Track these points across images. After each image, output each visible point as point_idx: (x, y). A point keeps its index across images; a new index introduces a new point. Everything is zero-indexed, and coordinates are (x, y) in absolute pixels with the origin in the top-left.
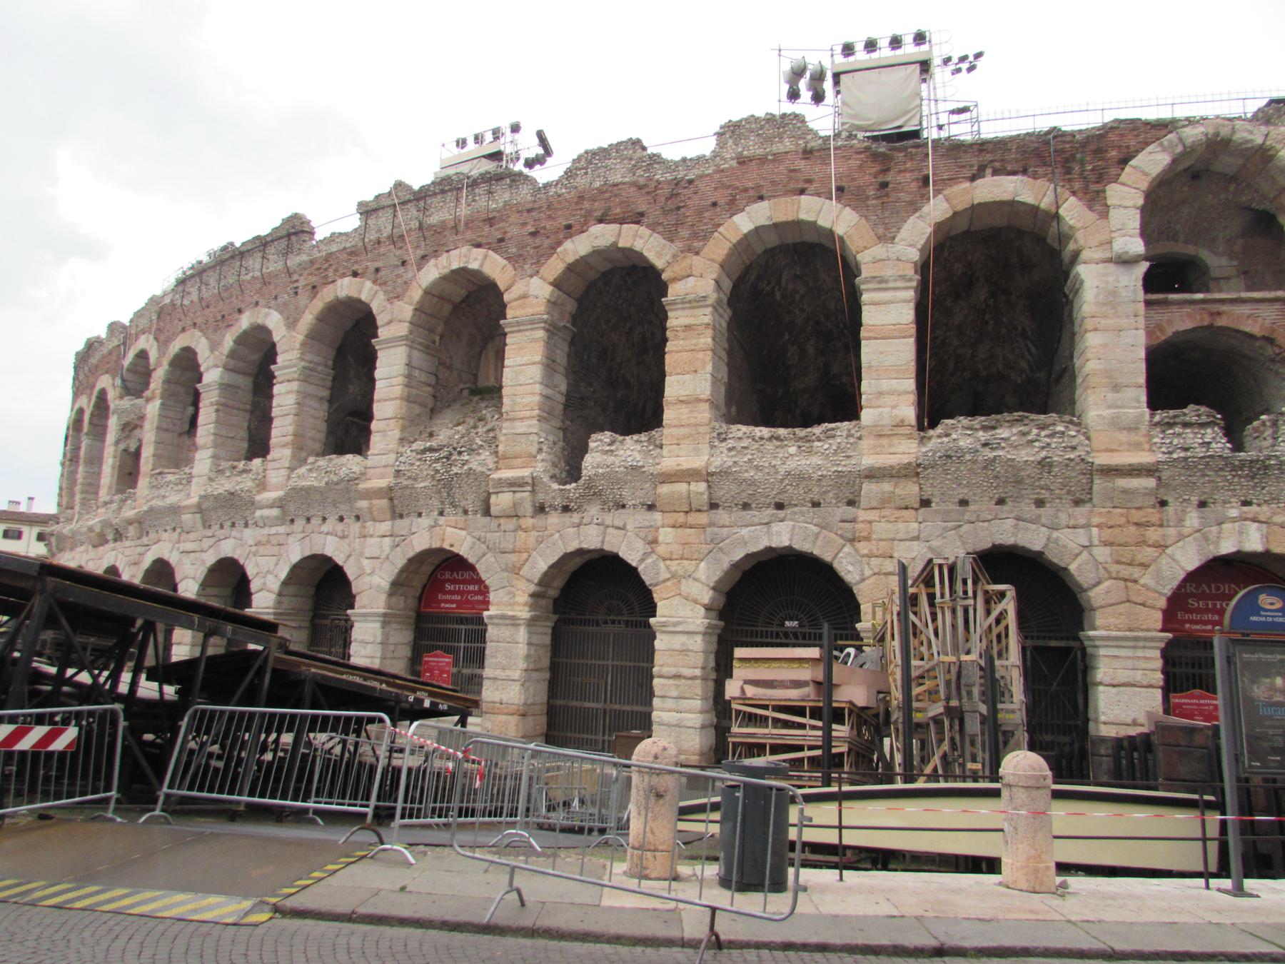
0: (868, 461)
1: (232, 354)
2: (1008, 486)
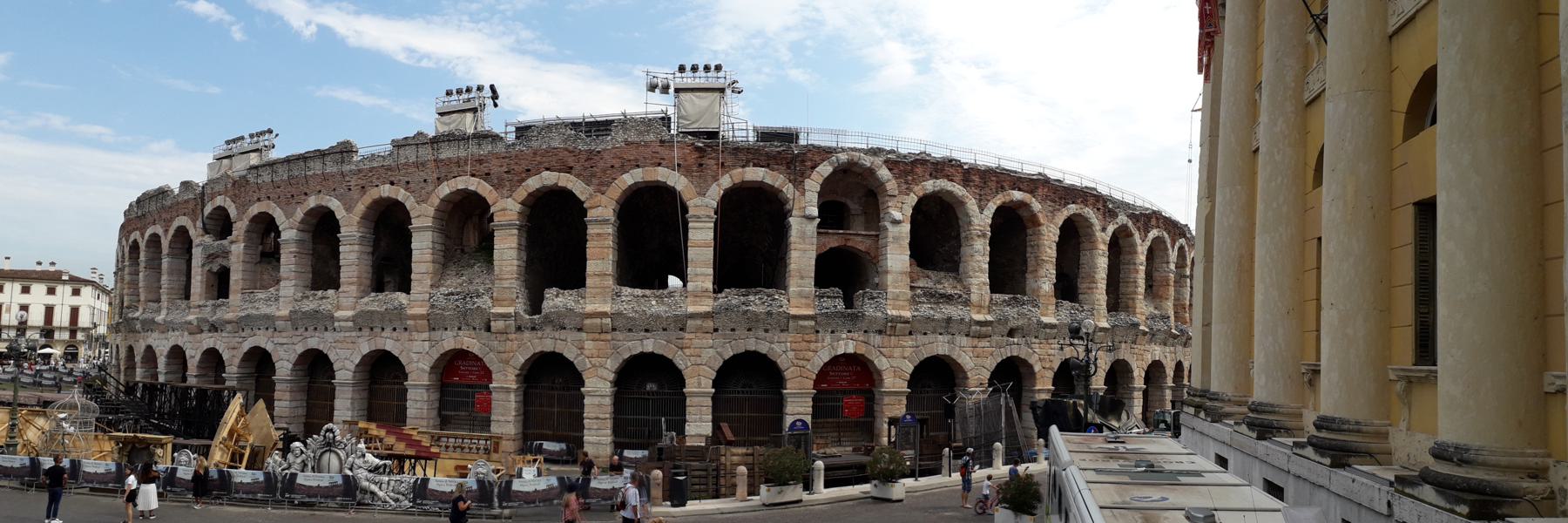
0: (691, 309)
1: (302, 222)
2: (753, 323)
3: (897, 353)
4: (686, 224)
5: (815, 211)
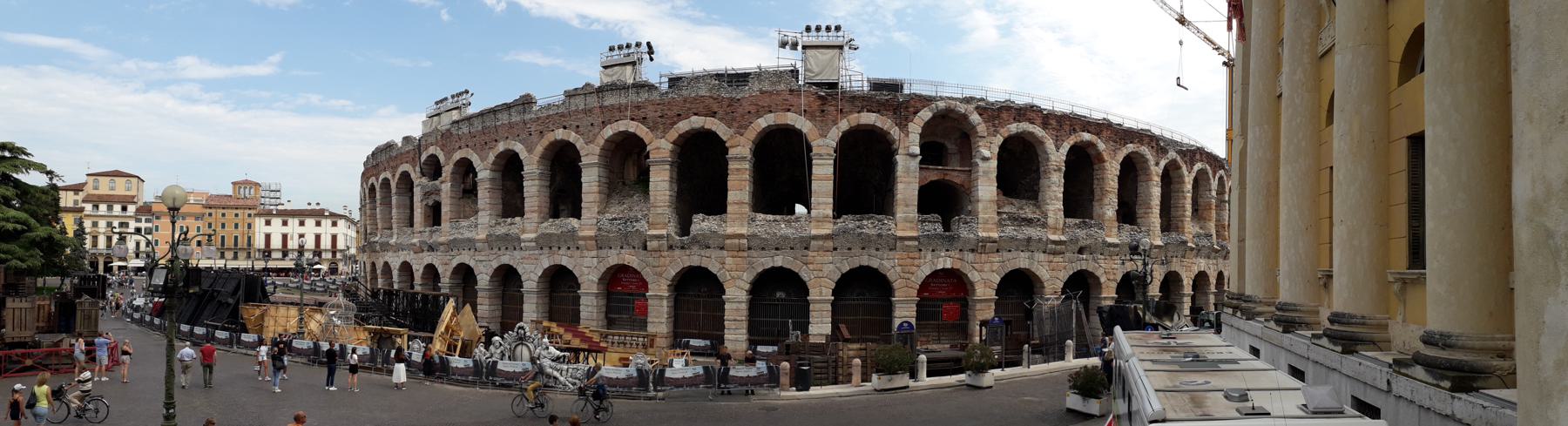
0: (814, 232)
2: (866, 243)
3: (987, 267)
4: (810, 160)
5: (917, 150)
